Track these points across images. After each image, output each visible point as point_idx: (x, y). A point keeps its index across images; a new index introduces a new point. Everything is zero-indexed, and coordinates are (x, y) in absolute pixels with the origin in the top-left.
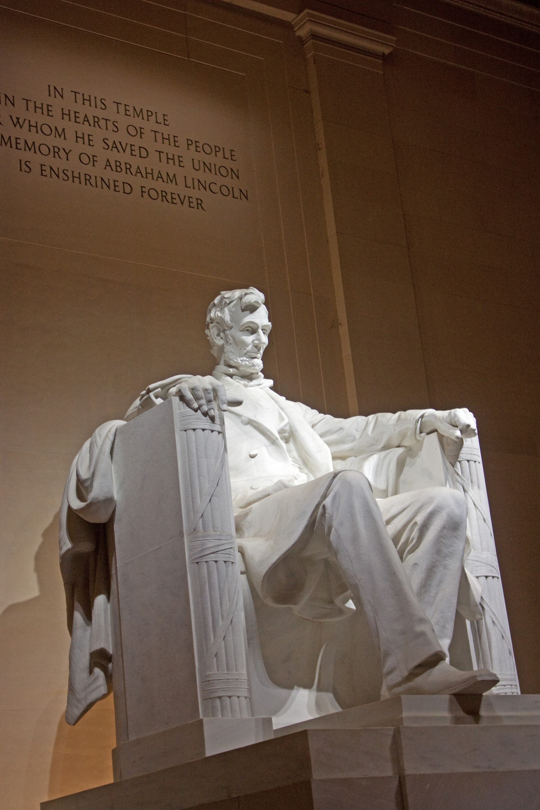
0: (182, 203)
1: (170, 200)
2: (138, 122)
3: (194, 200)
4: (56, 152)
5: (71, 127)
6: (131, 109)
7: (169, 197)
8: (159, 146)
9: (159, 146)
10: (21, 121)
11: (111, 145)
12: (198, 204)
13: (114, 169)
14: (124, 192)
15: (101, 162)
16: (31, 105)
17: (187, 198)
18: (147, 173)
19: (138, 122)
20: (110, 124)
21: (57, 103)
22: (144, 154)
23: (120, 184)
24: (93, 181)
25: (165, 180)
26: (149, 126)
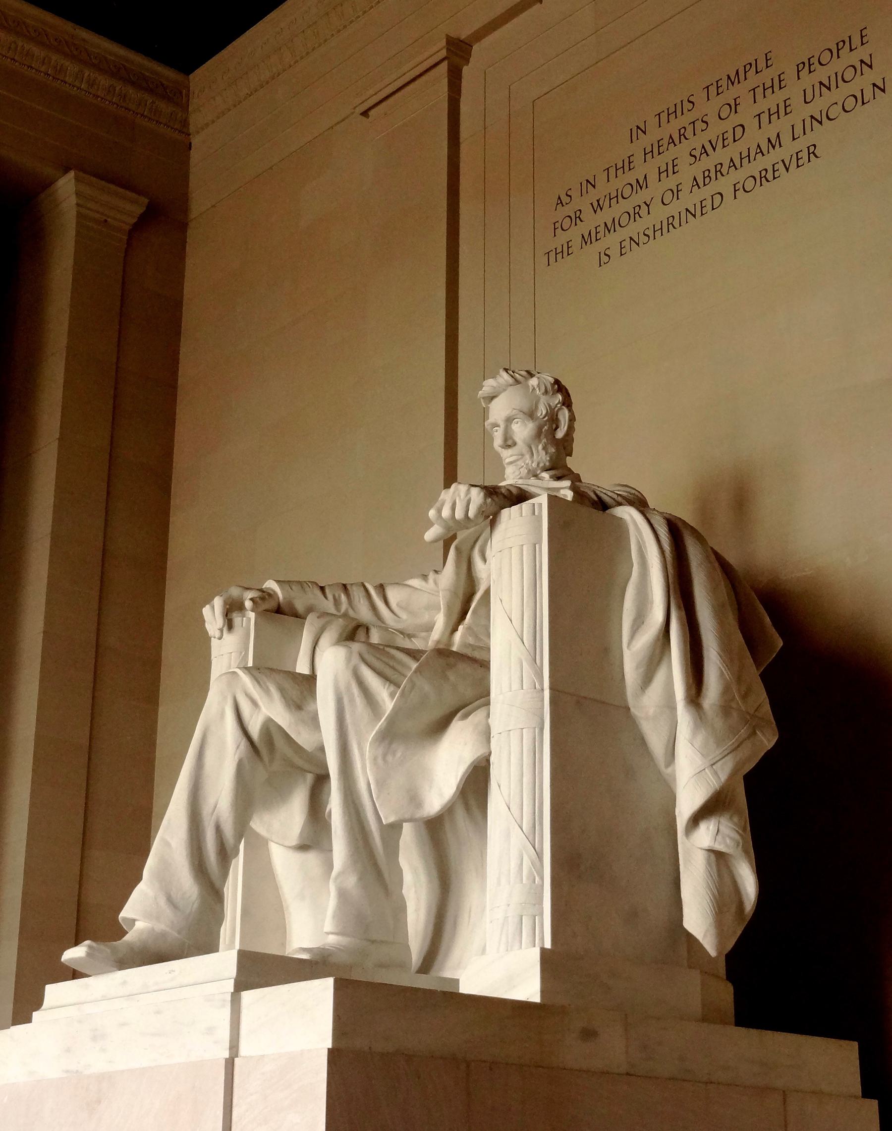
0: (787, 170)
2: (729, 96)
3: (804, 155)
6: (724, 83)
7: (770, 176)
10: (601, 203)
11: (697, 154)
12: (809, 154)
13: (701, 184)
14: (713, 209)
18: (741, 159)
20: (700, 125)
23: (708, 203)
24: (676, 223)
25: (765, 151)
26: (741, 90)
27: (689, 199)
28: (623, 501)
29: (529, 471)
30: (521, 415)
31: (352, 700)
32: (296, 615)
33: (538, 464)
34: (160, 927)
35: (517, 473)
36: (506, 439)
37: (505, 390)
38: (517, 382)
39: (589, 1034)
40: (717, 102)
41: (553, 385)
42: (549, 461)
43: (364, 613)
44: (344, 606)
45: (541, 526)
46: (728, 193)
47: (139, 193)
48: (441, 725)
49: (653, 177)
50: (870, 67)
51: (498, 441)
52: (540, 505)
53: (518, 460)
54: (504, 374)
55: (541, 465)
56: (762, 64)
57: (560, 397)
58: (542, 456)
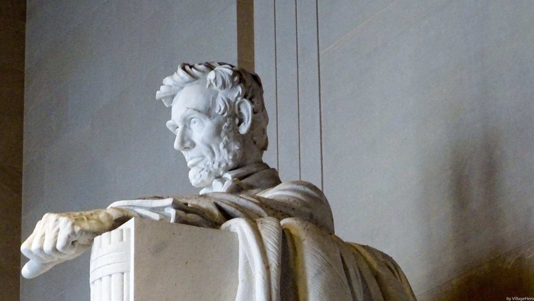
28: (238, 213)
29: (210, 173)
30: (196, 114)
33: (219, 165)
35: (198, 176)
36: (183, 142)
37: (182, 88)
41: (232, 77)
42: (233, 160)
45: (128, 253)
51: (176, 144)
52: (129, 230)
53: (199, 162)
54: (180, 71)
55: (223, 165)
57: (240, 89)
58: (224, 157)
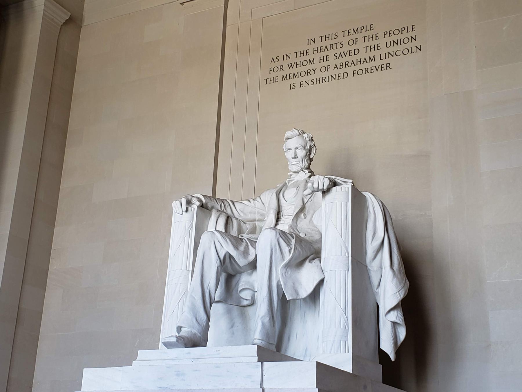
1: (370, 72)
4: (309, 72)
5: (317, 56)
8: (367, 44)
9: (367, 44)
10: (292, 65)
11: (338, 56)
13: (339, 68)
15: (332, 67)
16: (298, 54)
17: (380, 66)
19: (354, 36)
20: (339, 45)
21: (311, 48)
22: (357, 51)
24: (326, 80)
25: (368, 61)
26: (360, 36)
27: (332, 72)
30: (302, 147)
31: (276, 250)
32: (207, 209)
34: (195, 331)
38: (300, 134)
39: (365, 387)
40: (347, 39)
43: (229, 212)
44: (223, 208)
46: (351, 74)
47: (68, 11)
48: (301, 264)
49: (317, 60)
50: (415, 40)
56: (368, 28)
58: (306, 164)
